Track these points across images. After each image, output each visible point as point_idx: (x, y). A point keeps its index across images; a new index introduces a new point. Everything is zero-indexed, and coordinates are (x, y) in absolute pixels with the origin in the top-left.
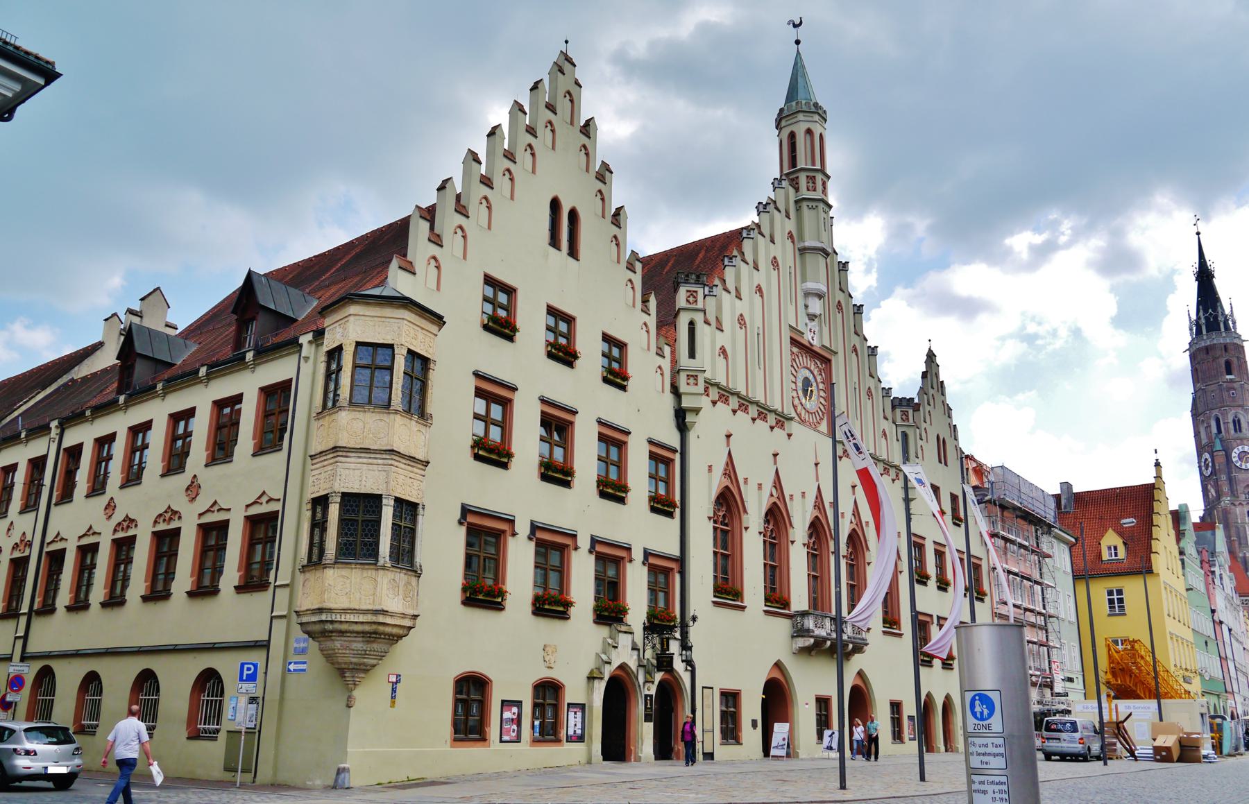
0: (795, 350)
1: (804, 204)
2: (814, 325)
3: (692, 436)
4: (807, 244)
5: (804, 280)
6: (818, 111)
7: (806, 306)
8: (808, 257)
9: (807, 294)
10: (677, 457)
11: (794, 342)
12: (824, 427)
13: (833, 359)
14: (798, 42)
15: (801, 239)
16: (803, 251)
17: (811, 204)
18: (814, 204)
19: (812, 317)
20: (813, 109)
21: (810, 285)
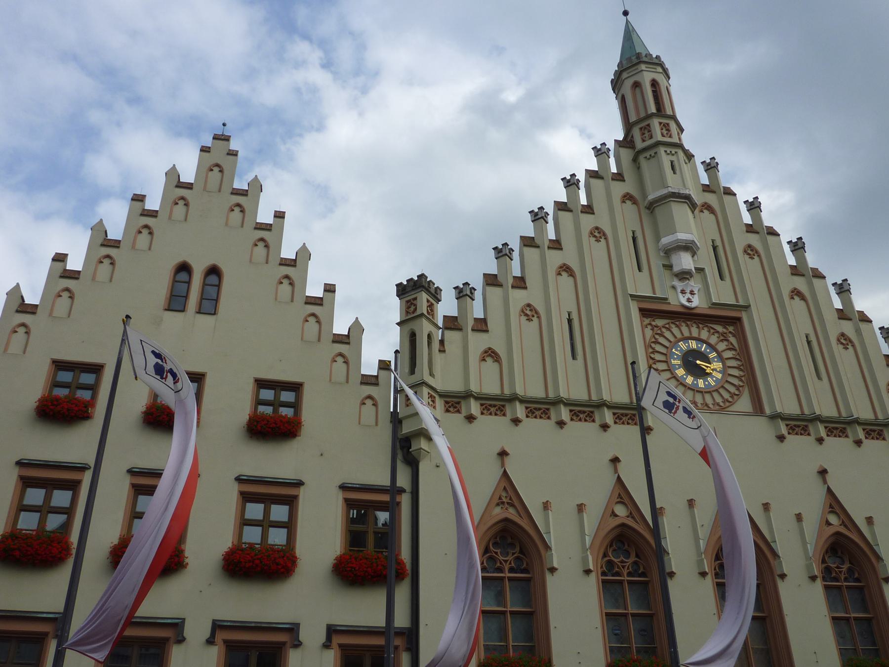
0: (660, 322)
1: (641, 158)
2: (694, 284)
3: (422, 467)
4: (651, 197)
5: (658, 239)
6: (657, 63)
7: (669, 267)
8: (658, 211)
9: (668, 252)
10: (405, 501)
11: (645, 313)
12: (744, 403)
13: (744, 316)
14: (626, 13)
15: (644, 195)
16: (651, 207)
17: (647, 154)
18: (652, 152)
19: (684, 275)
20: (635, 60)
21: (665, 240)
